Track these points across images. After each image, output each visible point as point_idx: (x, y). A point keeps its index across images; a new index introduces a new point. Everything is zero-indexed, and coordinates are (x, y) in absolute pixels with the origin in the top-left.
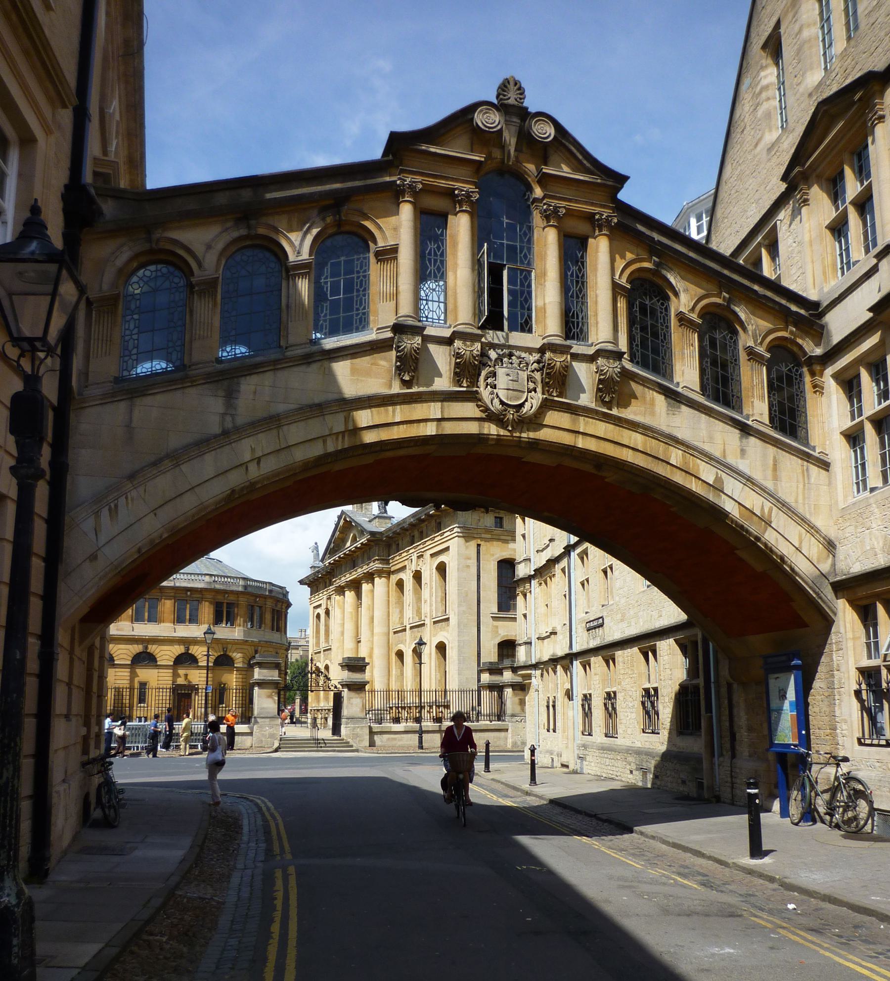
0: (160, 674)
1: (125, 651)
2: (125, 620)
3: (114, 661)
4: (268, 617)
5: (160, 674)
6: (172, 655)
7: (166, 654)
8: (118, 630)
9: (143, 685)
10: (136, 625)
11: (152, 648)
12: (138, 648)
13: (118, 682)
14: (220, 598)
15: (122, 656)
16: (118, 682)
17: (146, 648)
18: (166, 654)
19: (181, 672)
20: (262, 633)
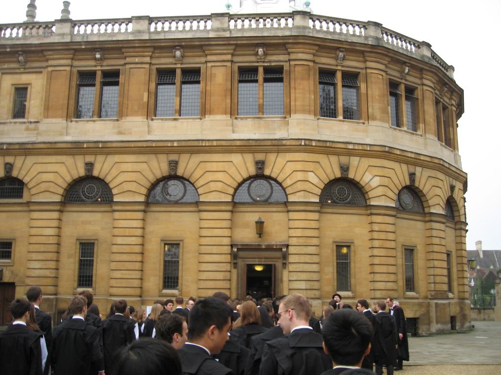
0: (205, 224)
1: (132, 177)
2: (135, 113)
3: (112, 195)
4: (429, 110)
5: (205, 224)
6: (229, 181)
7: (217, 177)
8: (120, 133)
9: (173, 246)
10: (156, 124)
11: (188, 165)
12: (158, 167)
13: (119, 240)
14: (327, 61)
15: (126, 187)
16: (119, 240)
17: (174, 164)
18: (217, 177)
19: (250, 217)
20: (421, 140)
